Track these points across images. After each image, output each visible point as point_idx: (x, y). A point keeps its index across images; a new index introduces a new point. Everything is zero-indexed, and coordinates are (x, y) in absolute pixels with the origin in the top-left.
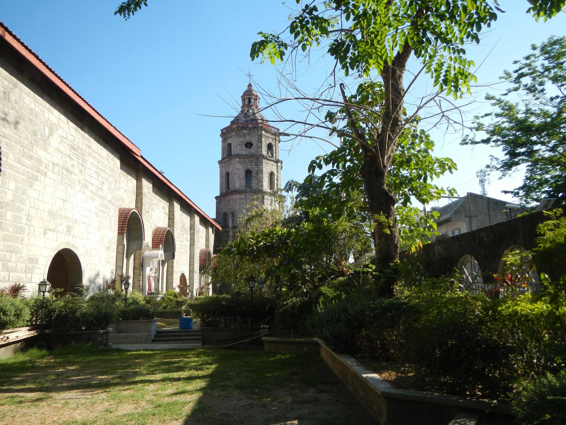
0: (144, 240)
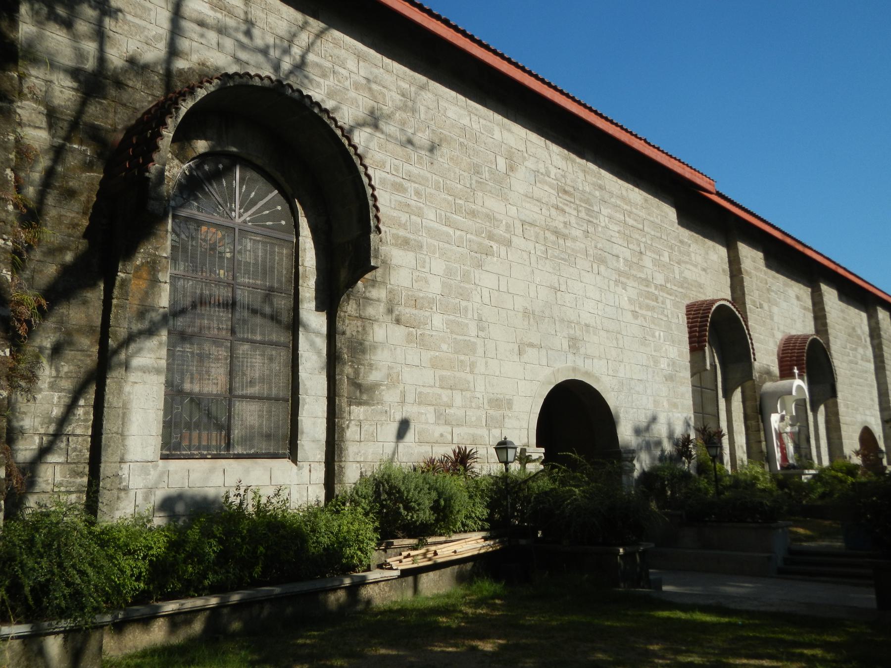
0: (755, 360)
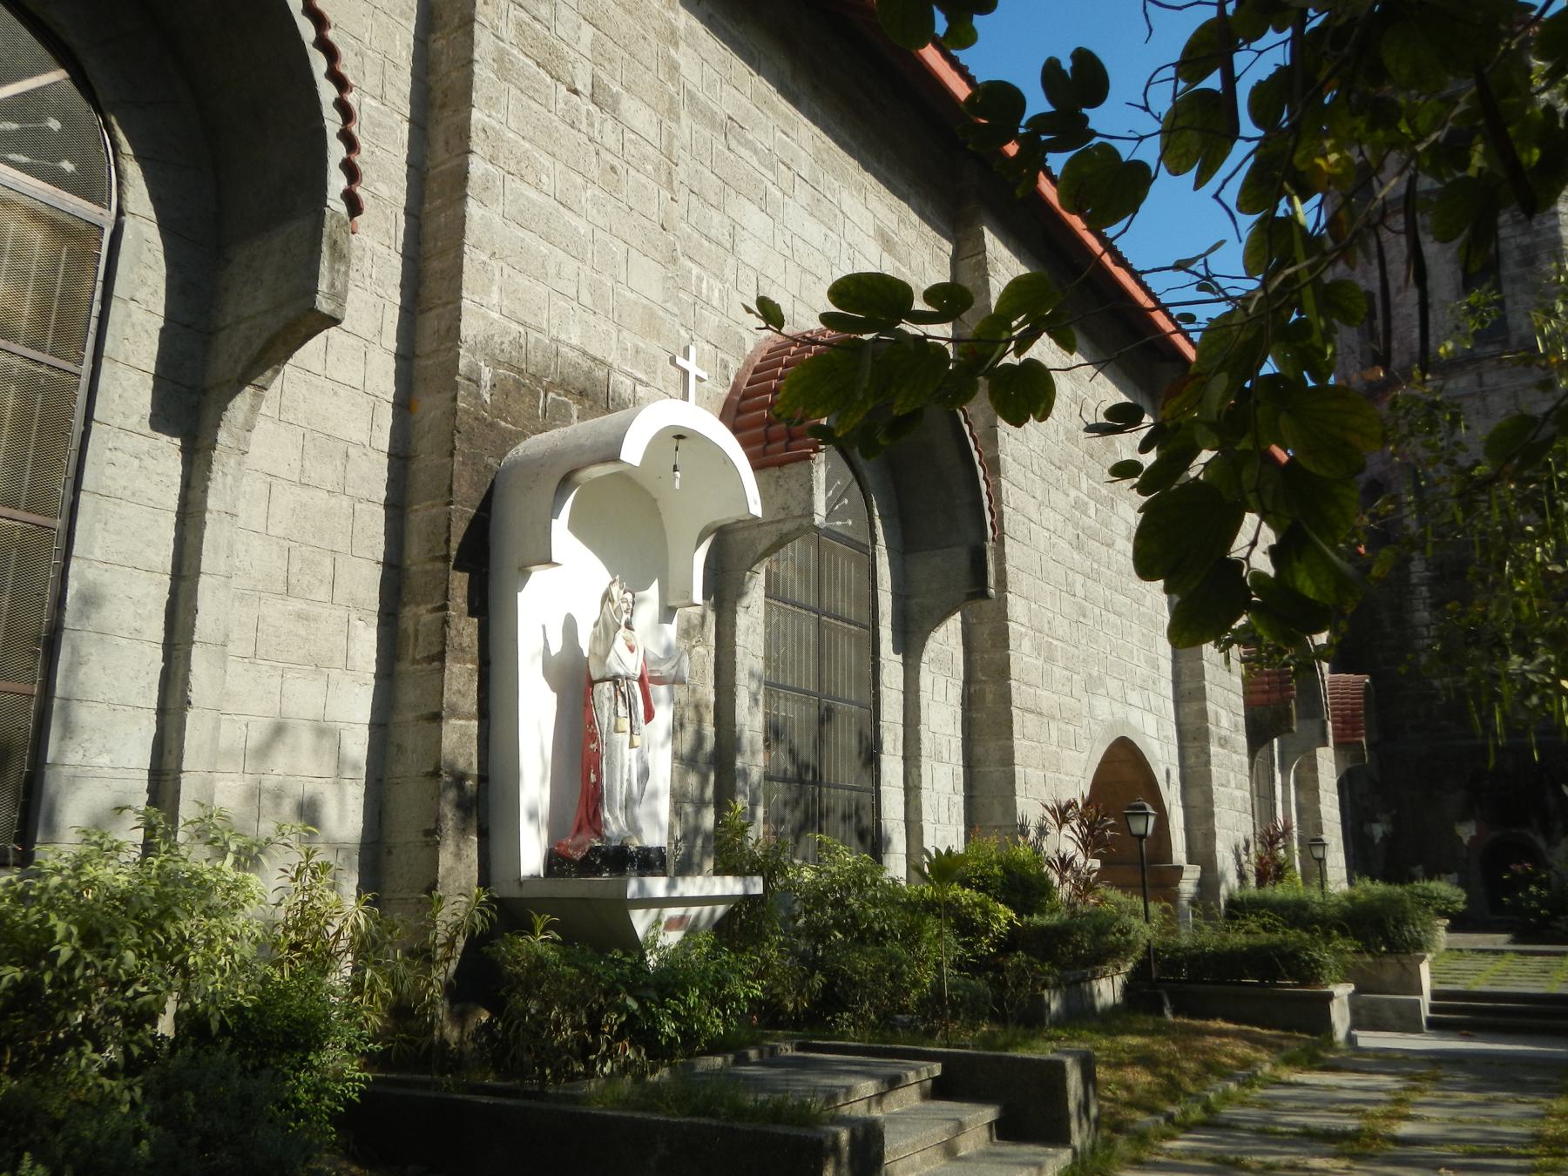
0: (353, 204)
